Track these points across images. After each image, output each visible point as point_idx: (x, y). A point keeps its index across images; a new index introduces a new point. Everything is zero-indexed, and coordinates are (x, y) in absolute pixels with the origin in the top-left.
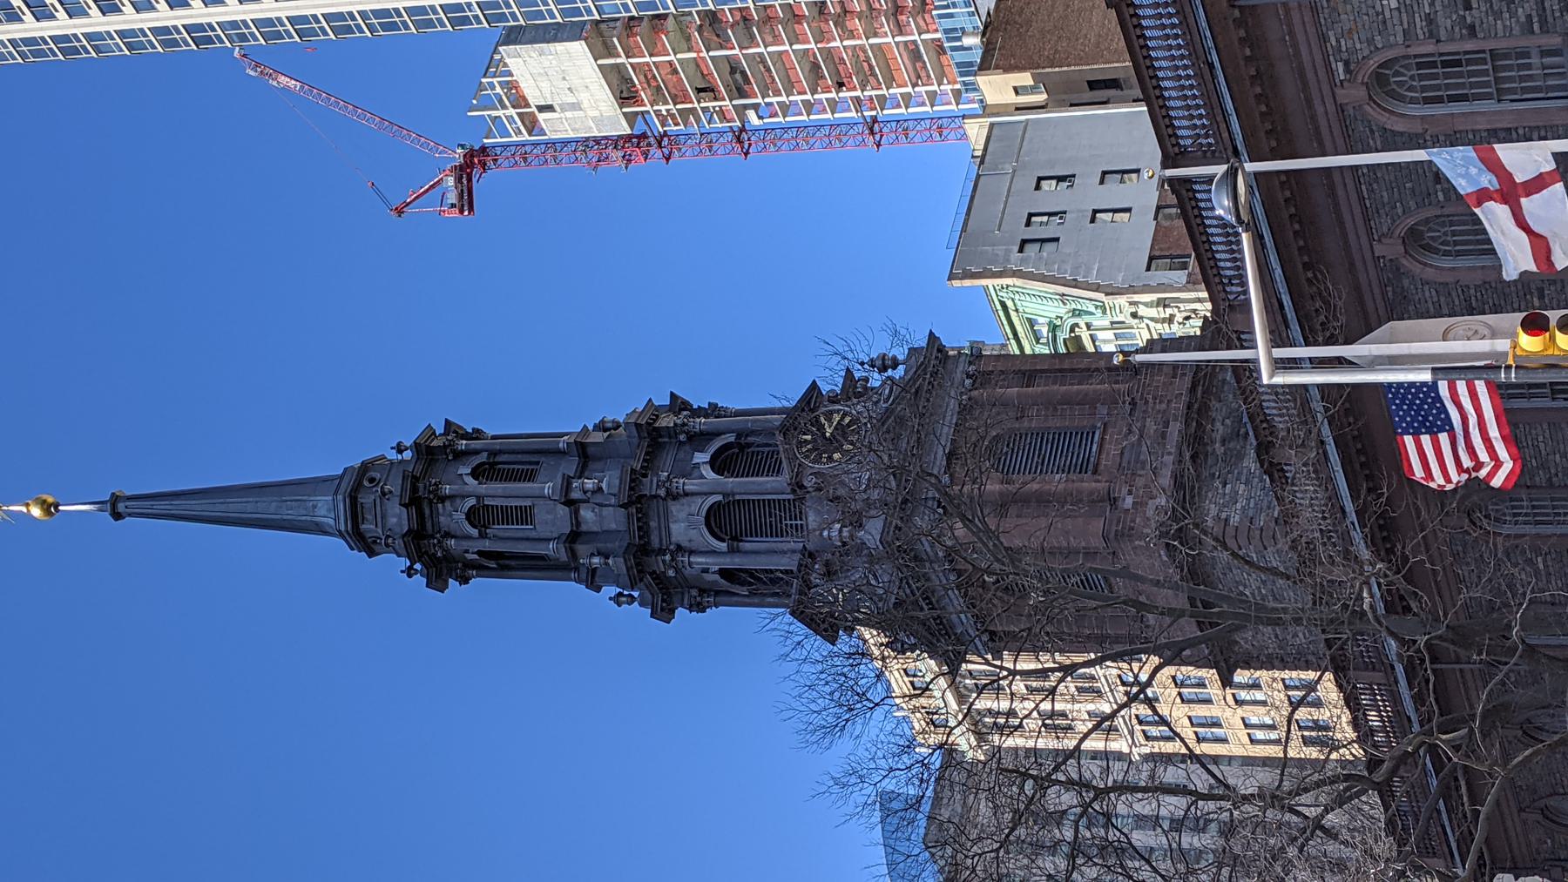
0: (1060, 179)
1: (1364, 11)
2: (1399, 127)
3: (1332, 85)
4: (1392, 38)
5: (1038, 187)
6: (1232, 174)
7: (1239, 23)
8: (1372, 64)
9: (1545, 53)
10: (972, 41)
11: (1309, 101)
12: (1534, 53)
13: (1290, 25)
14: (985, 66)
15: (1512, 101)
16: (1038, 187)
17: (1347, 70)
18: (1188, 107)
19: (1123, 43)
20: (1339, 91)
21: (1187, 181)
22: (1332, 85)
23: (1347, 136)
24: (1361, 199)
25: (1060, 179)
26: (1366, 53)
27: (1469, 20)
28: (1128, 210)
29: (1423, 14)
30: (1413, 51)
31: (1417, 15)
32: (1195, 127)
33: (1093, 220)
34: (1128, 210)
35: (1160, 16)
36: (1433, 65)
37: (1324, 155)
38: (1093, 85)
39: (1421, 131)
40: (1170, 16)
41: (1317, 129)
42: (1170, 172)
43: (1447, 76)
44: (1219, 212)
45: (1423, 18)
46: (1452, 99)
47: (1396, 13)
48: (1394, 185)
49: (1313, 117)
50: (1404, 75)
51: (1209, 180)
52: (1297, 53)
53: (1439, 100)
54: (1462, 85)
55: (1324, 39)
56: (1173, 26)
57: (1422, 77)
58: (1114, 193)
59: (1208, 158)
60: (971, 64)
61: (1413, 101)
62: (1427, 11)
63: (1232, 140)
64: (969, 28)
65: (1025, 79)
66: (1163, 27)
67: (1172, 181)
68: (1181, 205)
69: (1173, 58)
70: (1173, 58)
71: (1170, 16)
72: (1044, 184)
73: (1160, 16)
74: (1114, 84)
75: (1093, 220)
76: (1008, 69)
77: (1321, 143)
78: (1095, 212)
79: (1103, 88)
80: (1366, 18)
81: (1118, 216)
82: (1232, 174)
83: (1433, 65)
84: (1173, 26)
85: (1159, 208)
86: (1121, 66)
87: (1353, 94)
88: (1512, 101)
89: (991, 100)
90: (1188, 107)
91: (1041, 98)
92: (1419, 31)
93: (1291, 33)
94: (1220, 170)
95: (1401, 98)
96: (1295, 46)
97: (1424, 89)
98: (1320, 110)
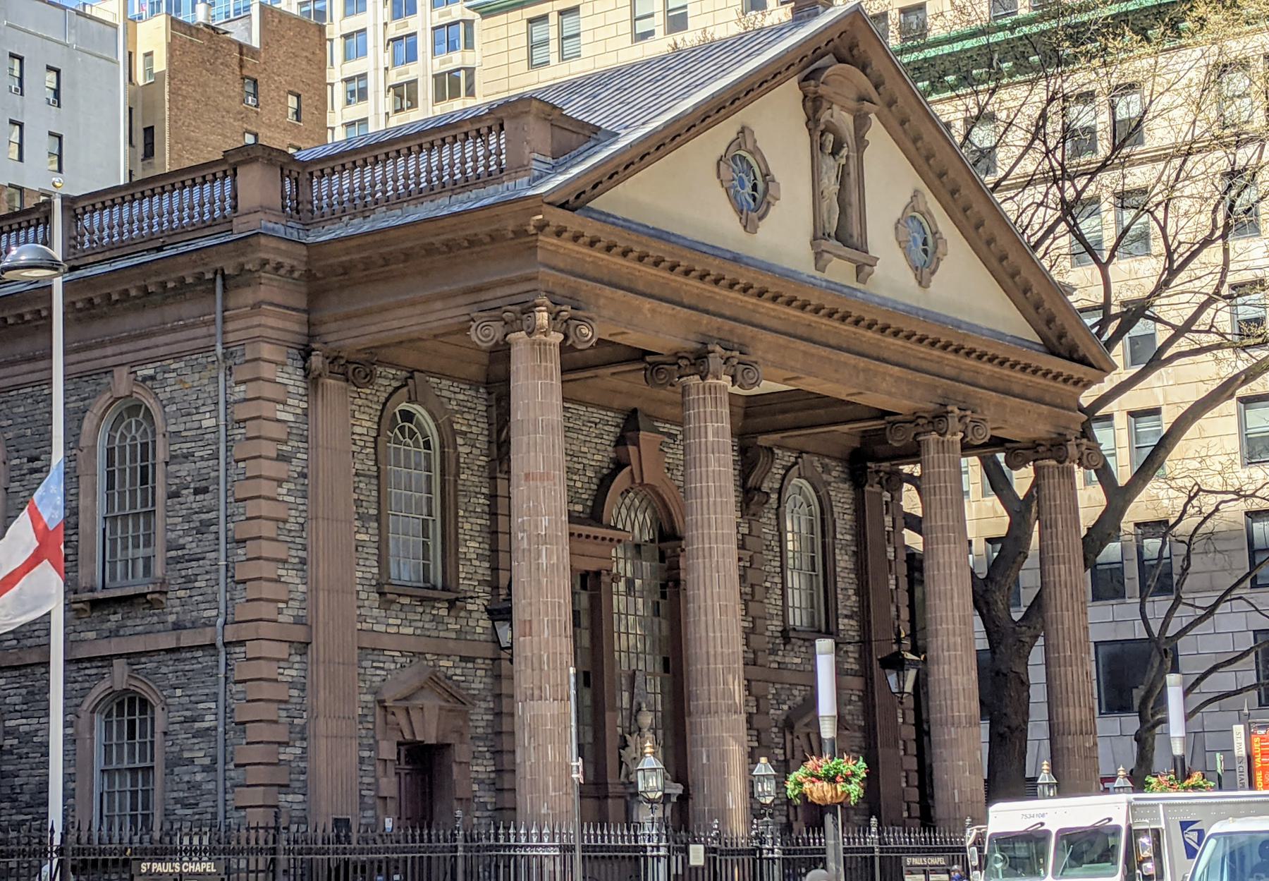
0: (57, 92)
1: (201, 396)
2: (87, 425)
3: (133, 364)
4: (173, 421)
5: (49, 68)
6: (53, 265)
7: (200, 278)
8: (150, 402)
9: (147, 560)
10: (201, 15)
11: (119, 341)
12: (149, 551)
13: (194, 326)
14: (175, 24)
15: (104, 530)
16: (49, 68)
17: (145, 379)
18: (121, 225)
19: (187, 164)
20: (126, 369)
21: (47, 220)
22: (133, 364)
23: (81, 376)
24: (17, 387)
25: (57, 92)
26: (161, 396)
27: (184, 492)
28: (21, 159)
29: (194, 450)
30: (159, 438)
31: (193, 444)
32: (101, 230)
33: (12, 122)
34: (21, 159)
35: (212, 203)
36: (144, 457)
37: (65, 353)
38: (149, 132)
39: (81, 445)
40: (212, 212)
41: (89, 348)
42: (57, 203)
43: (133, 470)
44: (14, 251)
45: (190, 450)
46: (111, 475)
47: (196, 425)
48: (29, 418)
49: (102, 345)
50: (137, 431)
51: (47, 242)
52: (165, 332)
53: (110, 462)
54: (123, 483)
55: (178, 357)
56: (201, 214)
57: (133, 447)
58: (39, 147)
59: (72, 242)
60: (178, 10)
61: (111, 439)
62: (196, 454)
63: (86, 266)
64: (214, 11)
65: (160, 65)
66: (202, 205)
67: (49, 203)
68: (23, 212)
69: (171, 213)
70: (171, 213)
71: (212, 212)
72: (53, 75)
73: (212, 203)
74: (149, 152)
75: (12, 122)
76: (171, 48)
77: (77, 350)
78: (21, 125)
79: (147, 142)
80: (195, 397)
81: (15, 148)
82: (53, 265)
83: (144, 457)
84: (201, 214)
85: (21, 189)
86: (166, 161)
87: (122, 383)
88: (104, 530)
89: (141, 27)
90: (121, 225)
91: (140, 79)
92: (177, 446)
93: (186, 327)
94: (57, 253)
95: (114, 427)
96: (174, 330)
97: (123, 448)
98: (109, 350)
